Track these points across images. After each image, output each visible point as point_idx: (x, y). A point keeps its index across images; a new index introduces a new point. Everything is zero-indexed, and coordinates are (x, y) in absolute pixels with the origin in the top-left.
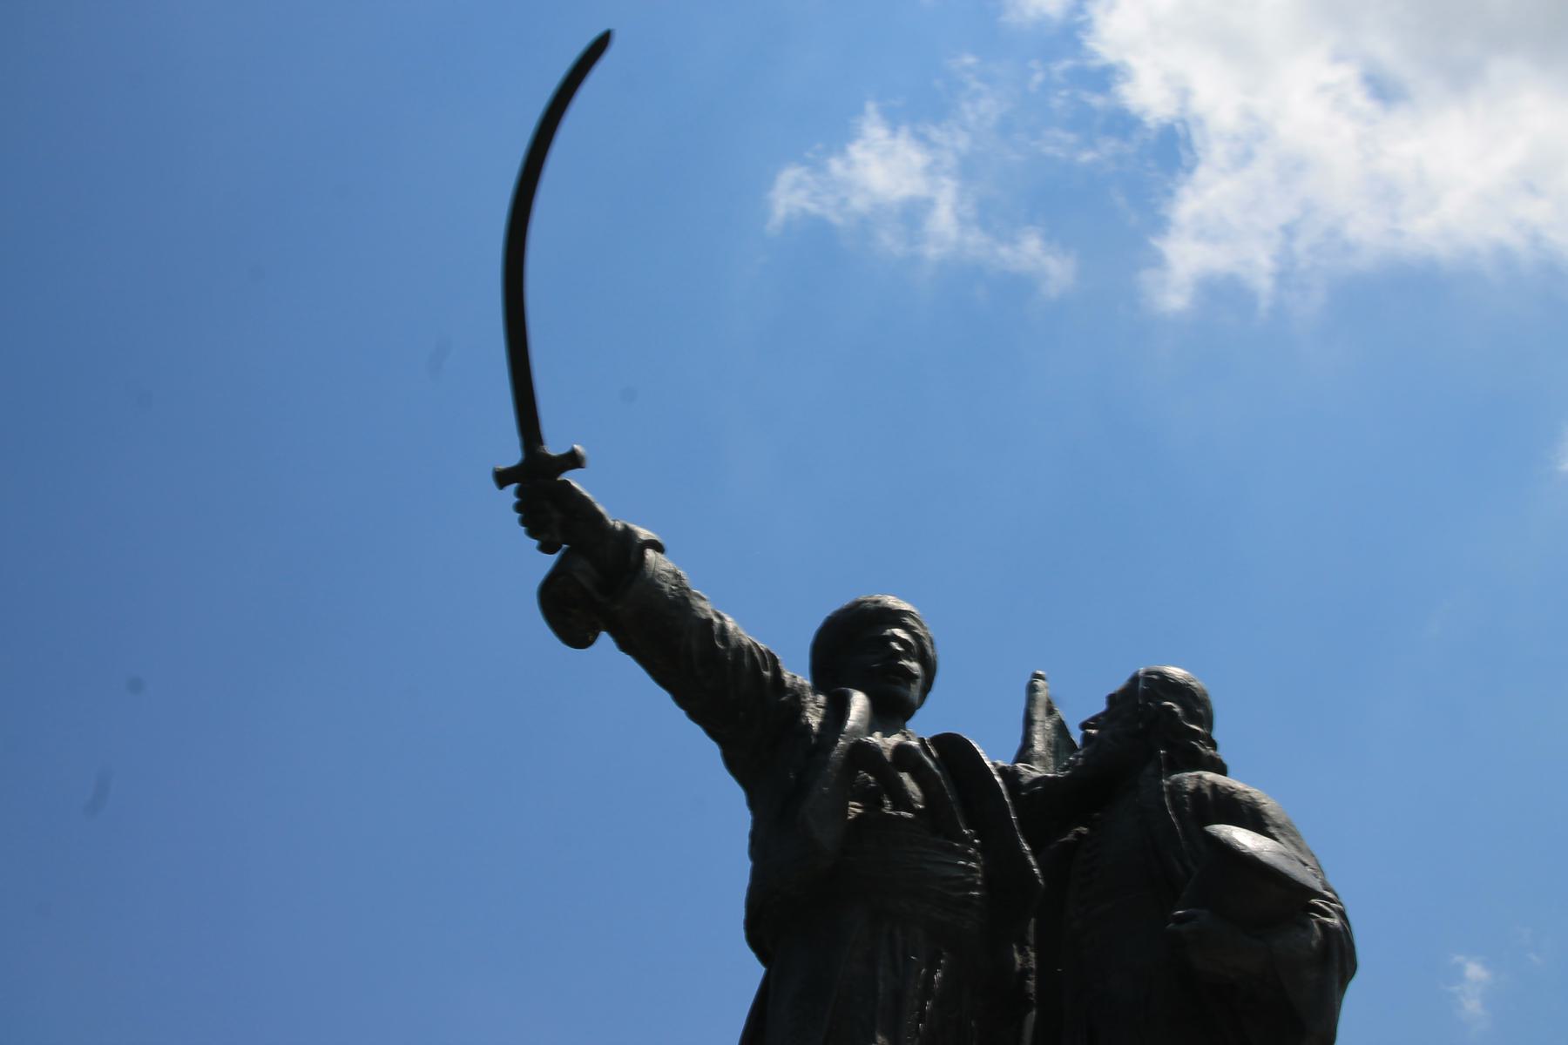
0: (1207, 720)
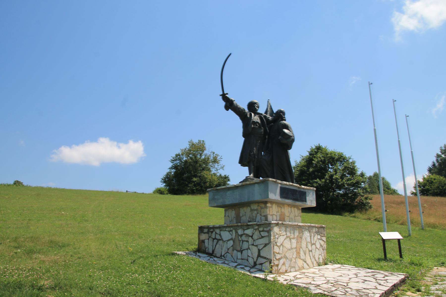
0: (284, 115)
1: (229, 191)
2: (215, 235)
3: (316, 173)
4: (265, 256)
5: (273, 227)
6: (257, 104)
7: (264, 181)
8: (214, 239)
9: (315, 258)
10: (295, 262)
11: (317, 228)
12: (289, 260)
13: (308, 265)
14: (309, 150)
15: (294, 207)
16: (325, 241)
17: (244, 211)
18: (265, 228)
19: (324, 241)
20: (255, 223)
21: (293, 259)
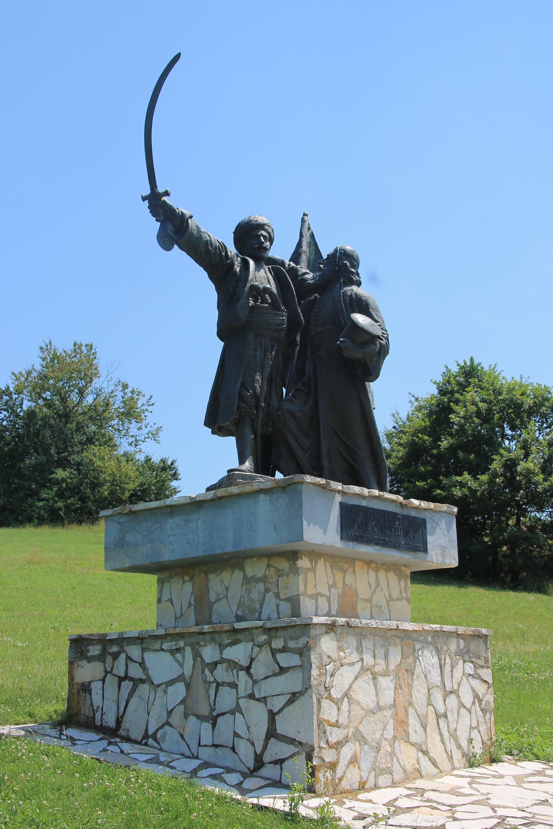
0: (356, 266)
1: (172, 517)
2: (127, 667)
3: (461, 454)
4: (291, 734)
5: (317, 638)
6: (266, 230)
7: (289, 485)
8: (121, 680)
9: (456, 740)
10: (392, 754)
11: (462, 639)
12: (371, 747)
13: (434, 764)
14: (439, 379)
15: (387, 570)
16: (490, 681)
17: (222, 582)
18: (291, 639)
19: (486, 681)
20: (259, 623)
21: (384, 743)
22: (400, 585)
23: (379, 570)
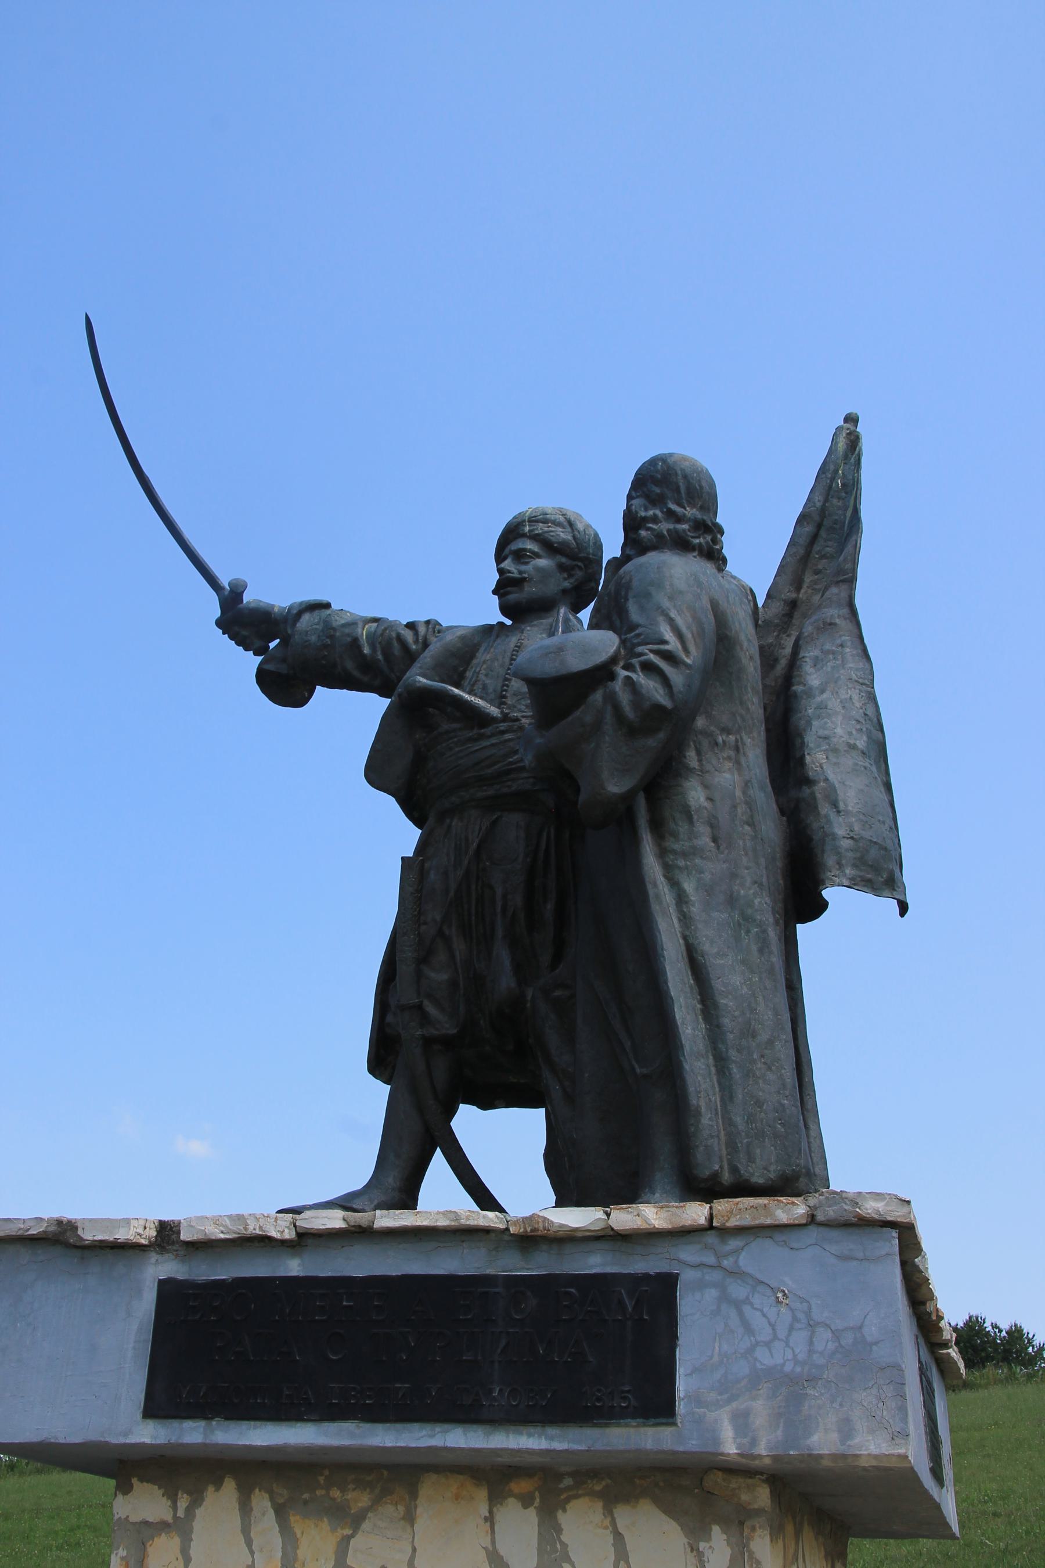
22: (700, 1555)
23: (568, 1500)
